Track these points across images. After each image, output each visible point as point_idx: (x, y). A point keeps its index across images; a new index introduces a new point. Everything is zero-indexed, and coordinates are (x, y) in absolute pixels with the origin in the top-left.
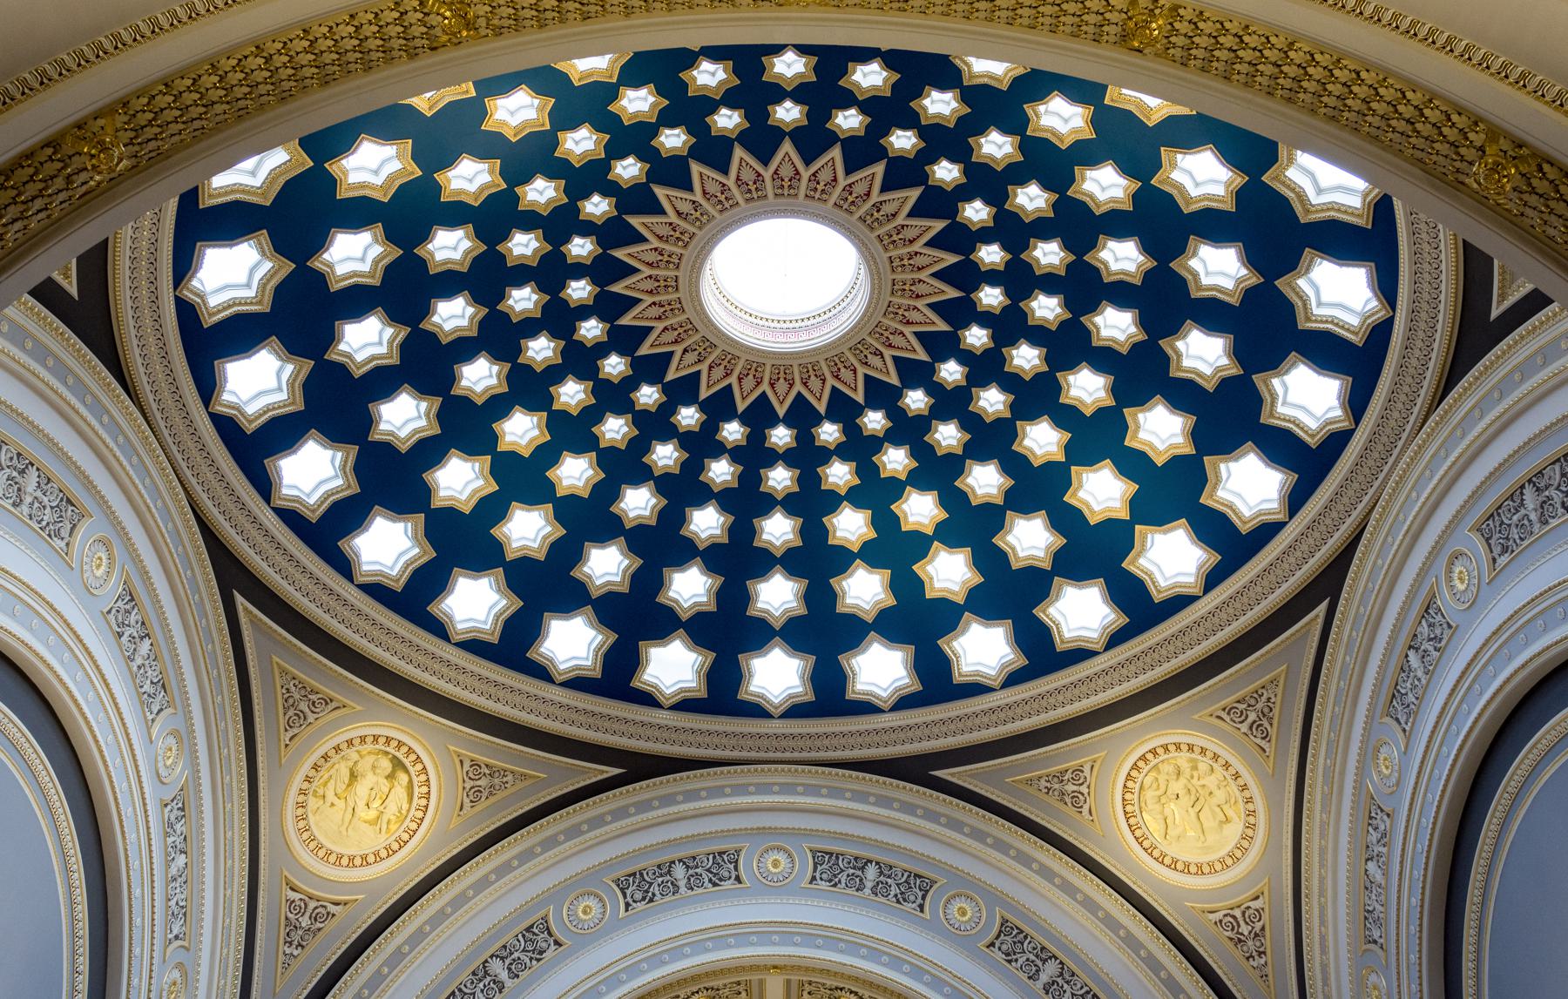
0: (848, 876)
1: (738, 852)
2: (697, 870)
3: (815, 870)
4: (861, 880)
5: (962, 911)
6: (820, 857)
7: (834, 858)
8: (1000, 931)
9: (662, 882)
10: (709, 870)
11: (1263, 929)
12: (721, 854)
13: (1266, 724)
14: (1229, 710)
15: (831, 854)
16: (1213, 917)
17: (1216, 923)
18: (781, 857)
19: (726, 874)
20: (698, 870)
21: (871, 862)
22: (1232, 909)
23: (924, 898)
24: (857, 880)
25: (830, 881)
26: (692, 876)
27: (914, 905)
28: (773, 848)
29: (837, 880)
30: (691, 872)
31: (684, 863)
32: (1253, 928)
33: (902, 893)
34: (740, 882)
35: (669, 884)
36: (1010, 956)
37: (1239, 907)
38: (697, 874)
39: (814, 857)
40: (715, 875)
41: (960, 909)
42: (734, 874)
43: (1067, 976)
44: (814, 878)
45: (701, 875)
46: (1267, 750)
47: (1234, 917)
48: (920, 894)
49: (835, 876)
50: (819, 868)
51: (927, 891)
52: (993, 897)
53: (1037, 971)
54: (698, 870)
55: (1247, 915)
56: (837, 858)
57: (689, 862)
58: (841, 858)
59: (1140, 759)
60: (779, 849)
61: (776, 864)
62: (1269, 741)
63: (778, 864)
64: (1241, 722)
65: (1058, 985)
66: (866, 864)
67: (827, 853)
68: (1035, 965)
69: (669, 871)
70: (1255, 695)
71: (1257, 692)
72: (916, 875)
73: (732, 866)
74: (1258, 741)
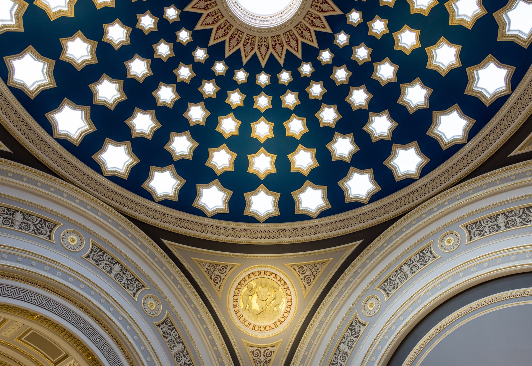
0: (106, 264)
1: (55, 225)
2: (29, 222)
3: (91, 253)
4: (111, 269)
5: (152, 304)
6: (95, 248)
7: (102, 252)
8: (164, 321)
9: (7, 218)
10: (35, 225)
11: (270, 360)
12: (45, 221)
13: (312, 278)
14: (300, 267)
15: (101, 250)
16: (251, 349)
17: (251, 352)
18: (76, 239)
19: (44, 232)
20: (30, 223)
21: (119, 263)
22: (261, 348)
23: (137, 291)
24: (109, 268)
25: (96, 261)
26: (25, 223)
27: (132, 292)
28: (74, 232)
29: (100, 263)
30: (25, 221)
31: (23, 215)
32: (266, 358)
33: (128, 284)
34: (50, 239)
35: (10, 221)
36: (165, 335)
37: (264, 348)
38: (27, 224)
39: (92, 247)
40: (38, 229)
41: (151, 303)
42: (48, 234)
43: (185, 353)
44: (88, 257)
45: (30, 225)
46: (307, 288)
47: (260, 352)
48: (136, 289)
49: (100, 261)
50: (93, 253)
51: (139, 289)
52: (167, 305)
53: (174, 346)
54: (30, 223)
55: (266, 352)
56: (104, 254)
57: (26, 216)
58: (105, 254)
59: (270, 272)
60: (77, 234)
61: (73, 240)
62: (309, 285)
63: (73, 240)
64: (302, 274)
65: (180, 355)
66: (116, 263)
67: (99, 248)
68: (174, 343)
69: (13, 214)
70: (314, 265)
71: (315, 264)
72: (136, 279)
73: (49, 230)
74: (305, 284)
